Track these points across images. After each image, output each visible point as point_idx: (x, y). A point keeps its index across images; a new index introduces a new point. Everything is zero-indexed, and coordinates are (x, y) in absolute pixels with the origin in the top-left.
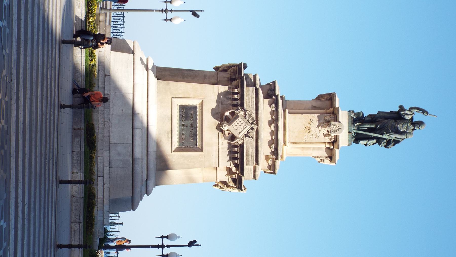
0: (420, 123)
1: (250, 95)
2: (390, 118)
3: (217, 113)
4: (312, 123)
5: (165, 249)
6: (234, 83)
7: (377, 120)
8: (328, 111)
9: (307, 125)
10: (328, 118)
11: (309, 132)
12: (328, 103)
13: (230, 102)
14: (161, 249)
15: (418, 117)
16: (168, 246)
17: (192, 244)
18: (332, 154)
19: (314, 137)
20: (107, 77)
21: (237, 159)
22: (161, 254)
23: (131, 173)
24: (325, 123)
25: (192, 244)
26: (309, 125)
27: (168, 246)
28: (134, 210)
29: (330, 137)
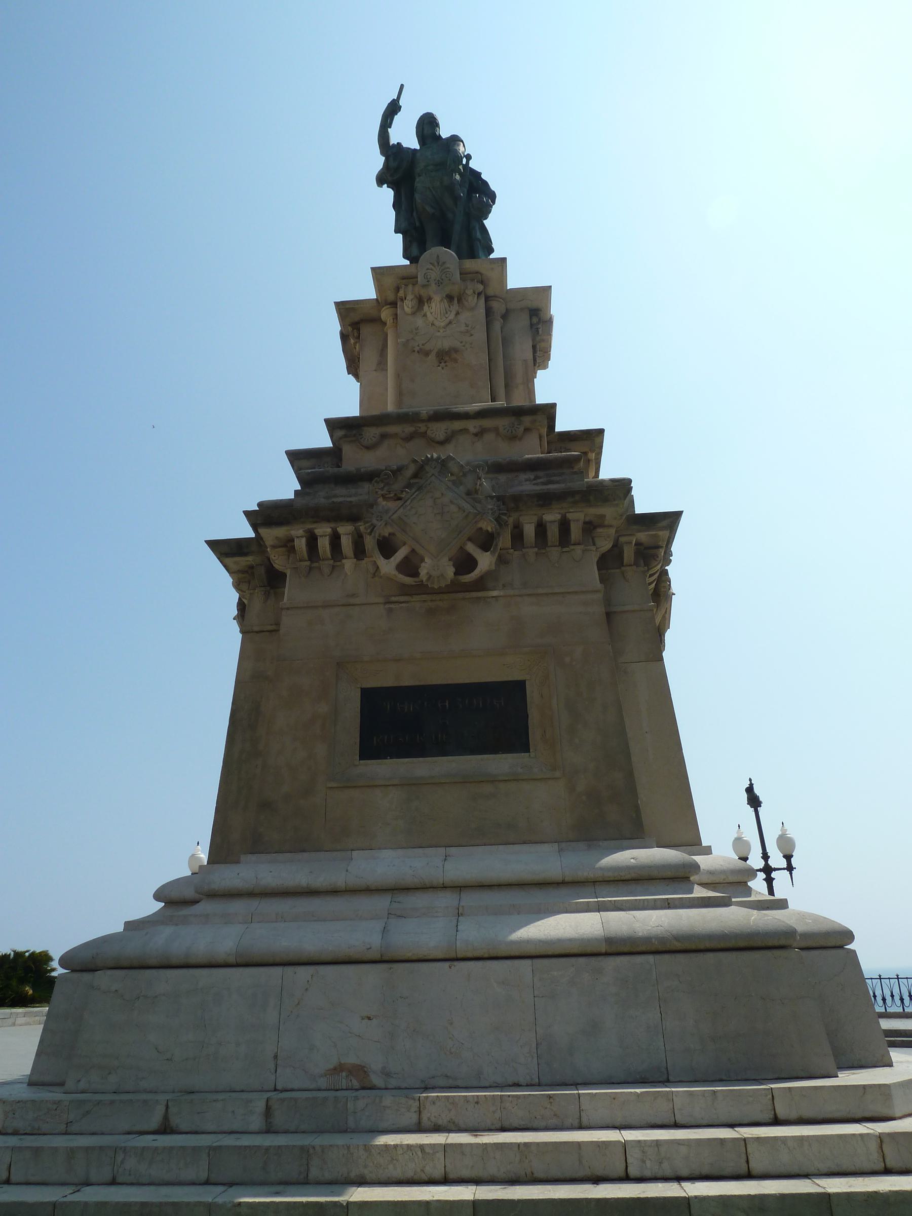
1: (323, 501)
2: (412, 191)
3: (390, 610)
4: (427, 347)
5: (772, 863)
6: (279, 562)
7: (418, 224)
8: (389, 321)
9: (432, 357)
10: (408, 306)
11: (456, 351)
12: (367, 331)
13: (349, 564)
14: (774, 875)
15: (405, 134)
16: (765, 857)
17: (754, 801)
18: (522, 309)
20: (175, 1121)
22: (787, 873)
23: (681, 957)
24: (426, 307)
25: (754, 801)
26: (433, 354)
27: (765, 857)
28: (849, 936)
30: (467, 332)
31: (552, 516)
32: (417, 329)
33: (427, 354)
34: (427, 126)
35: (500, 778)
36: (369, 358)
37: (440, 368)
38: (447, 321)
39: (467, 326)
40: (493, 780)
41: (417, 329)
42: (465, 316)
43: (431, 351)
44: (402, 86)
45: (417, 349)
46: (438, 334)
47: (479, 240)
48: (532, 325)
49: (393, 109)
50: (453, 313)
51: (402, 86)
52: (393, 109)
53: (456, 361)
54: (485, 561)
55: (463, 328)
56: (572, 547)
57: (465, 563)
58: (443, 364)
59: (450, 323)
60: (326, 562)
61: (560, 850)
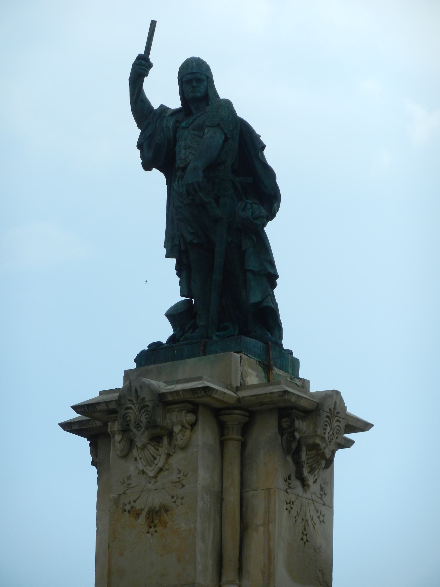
0: (195, 77)
4: (138, 506)
9: (142, 519)
11: (167, 511)
26: (144, 513)
29: (177, 429)
32: (129, 478)
33: (138, 515)
37: (149, 535)
38: (157, 469)
39: (180, 472)
41: (129, 478)
42: (178, 459)
43: (142, 510)
44: (153, 24)
45: (128, 508)
46: (150, 486)
49: (141, 67)
50: (163, 457)
51: (153, 24)
52: (141, 67)
53: (164, 524)
55: (174, 478)
58: (152, 530)
59: (161, 470)
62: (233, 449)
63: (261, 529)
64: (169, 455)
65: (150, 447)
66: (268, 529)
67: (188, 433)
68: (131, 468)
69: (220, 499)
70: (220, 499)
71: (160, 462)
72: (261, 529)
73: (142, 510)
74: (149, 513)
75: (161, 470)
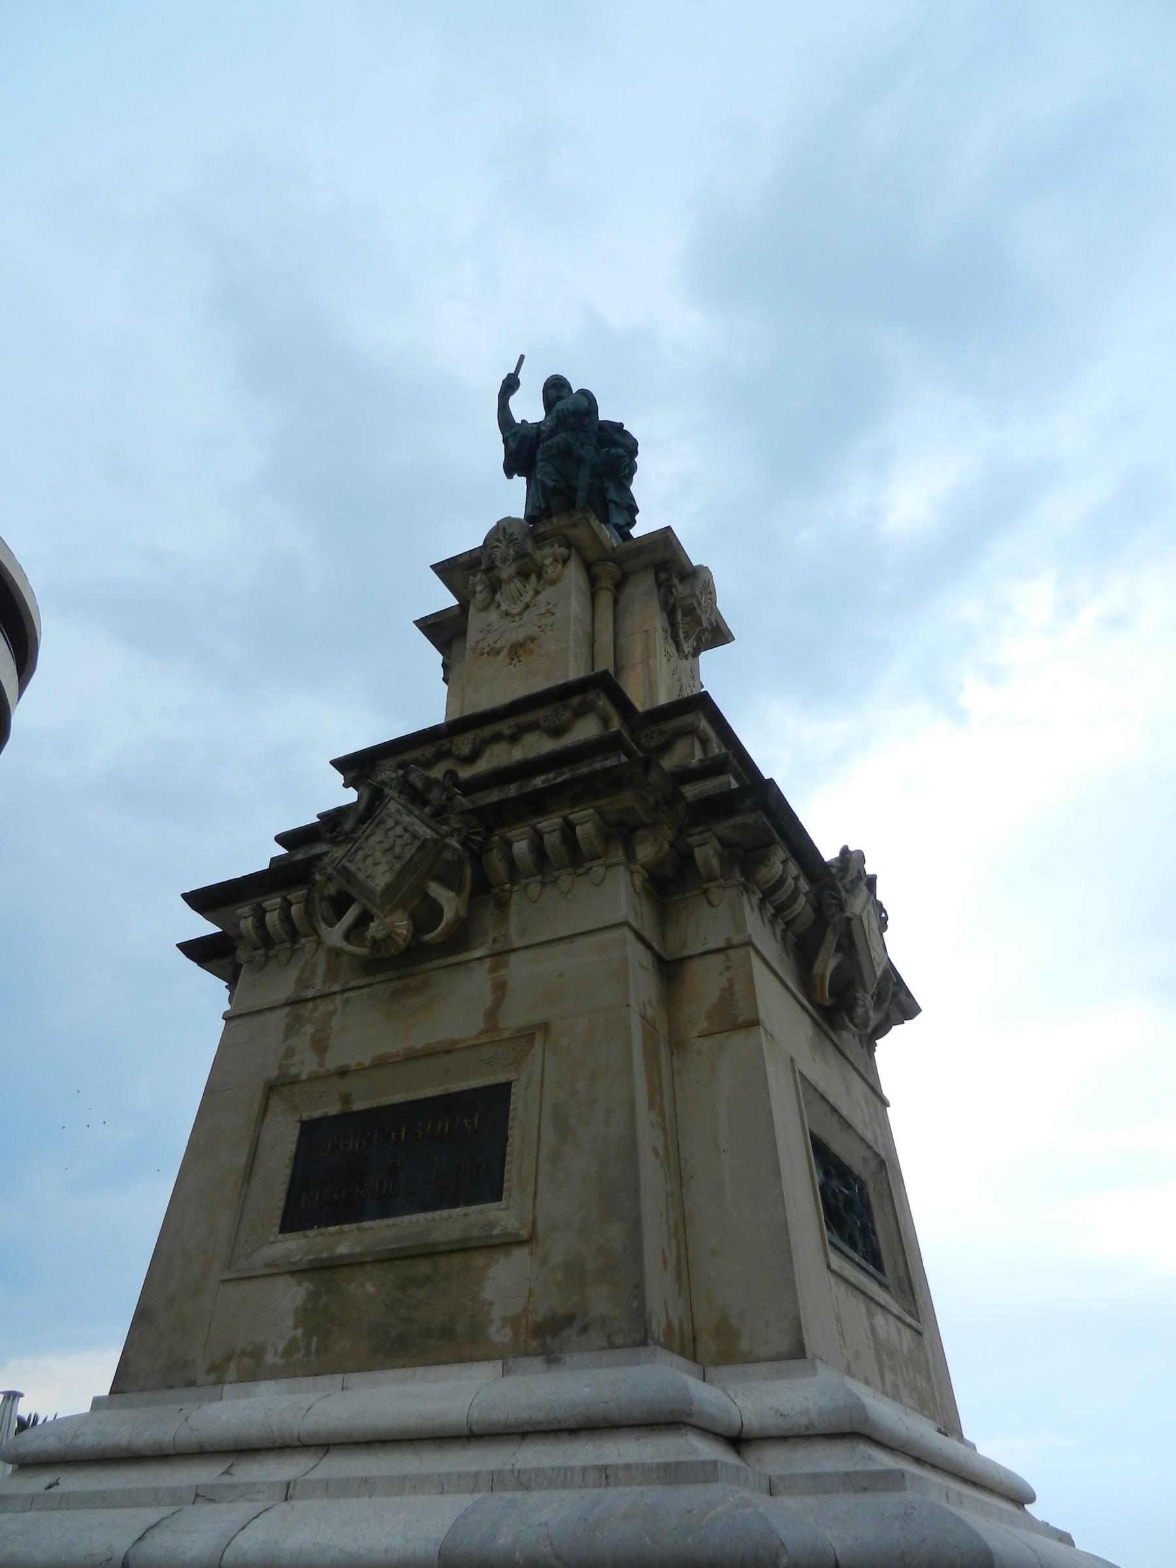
4: (498, 645)
11: (532, 639)
15: (529, 408)
19: (549, 620)
21: (569, 829)
30: (548, 611)
31: (550, 824)
32: (490, 625)
34: (555, 388)
35: (441, 1248)
36: (451, 677)
38: (522, 605)
39: (548, 604)
40: (431, 1253)
41: (490, 625)
42: (548, 594)
43: (502, 648)
44: (522, 358)
45: (487, 649)
47: (614, 502)
48: (659, 584)
49: (510, 385)
50: (531, 592)
51: (522, 358)
52: (510, 385)
54: (450, 903)
55: (543, 610)
56: (587, 865)
57: (427, 915)
59: (527, 606)
60: (283, 946)
61: (505, 1372)
62: (605, 598)
63: (639, 667)
64: (537, 592)
65: (516, 581)
66: (648, 664)
67: (560, 566)
68: (493, 615)
69: (592, 641)
70: (592, 641)
71: (527, 598)
72: (639, 667)
73: (502, 648)
74: (511, 647)
75: (527, 606)
